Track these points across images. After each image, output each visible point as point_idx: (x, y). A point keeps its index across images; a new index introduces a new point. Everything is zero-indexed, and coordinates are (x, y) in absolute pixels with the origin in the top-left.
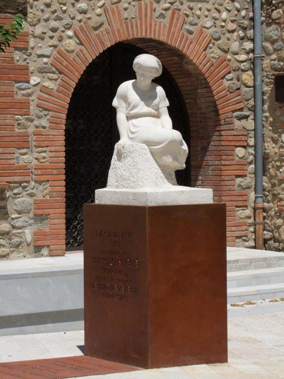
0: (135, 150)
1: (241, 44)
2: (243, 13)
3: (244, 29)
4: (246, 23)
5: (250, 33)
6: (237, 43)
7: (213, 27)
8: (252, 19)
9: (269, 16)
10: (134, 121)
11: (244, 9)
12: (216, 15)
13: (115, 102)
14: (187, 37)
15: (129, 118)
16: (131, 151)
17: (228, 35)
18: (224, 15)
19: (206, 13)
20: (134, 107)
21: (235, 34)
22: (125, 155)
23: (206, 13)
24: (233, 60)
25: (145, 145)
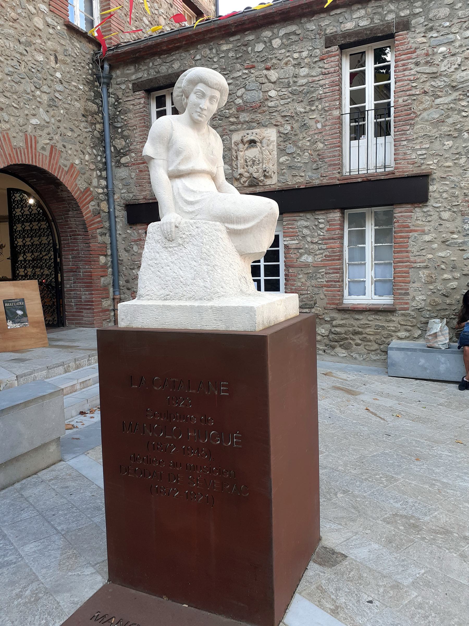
0: (202, 231)
1: (98, 181)
2: (99, 158)
3: (100, 170)
4: (101, 166)
5: (104, 173)
6: (96, 180)
7: (80, 164)
8: (105, 163)
9: (119, 161)
10: (186, 182)
11: (99, 155)
12: (82, 156)
13: (148, 149)
14: (63, 169)
15: (175, 175)
16: (194, 233)
17: (90, 172)
18: (87, 157)
19: (75, 153)
20: (187, 159)
21: (95, 173)
22: (180, 241)
23: (75, 153)
24: (94, 191)
25: (218, 223)
